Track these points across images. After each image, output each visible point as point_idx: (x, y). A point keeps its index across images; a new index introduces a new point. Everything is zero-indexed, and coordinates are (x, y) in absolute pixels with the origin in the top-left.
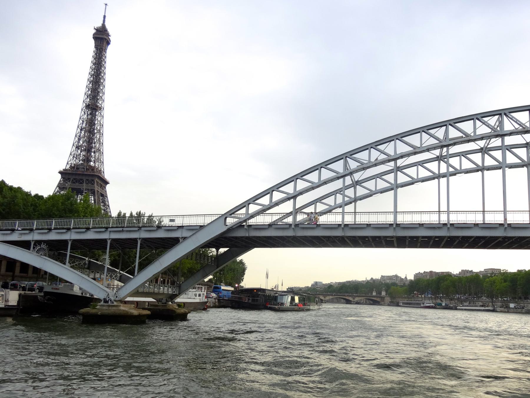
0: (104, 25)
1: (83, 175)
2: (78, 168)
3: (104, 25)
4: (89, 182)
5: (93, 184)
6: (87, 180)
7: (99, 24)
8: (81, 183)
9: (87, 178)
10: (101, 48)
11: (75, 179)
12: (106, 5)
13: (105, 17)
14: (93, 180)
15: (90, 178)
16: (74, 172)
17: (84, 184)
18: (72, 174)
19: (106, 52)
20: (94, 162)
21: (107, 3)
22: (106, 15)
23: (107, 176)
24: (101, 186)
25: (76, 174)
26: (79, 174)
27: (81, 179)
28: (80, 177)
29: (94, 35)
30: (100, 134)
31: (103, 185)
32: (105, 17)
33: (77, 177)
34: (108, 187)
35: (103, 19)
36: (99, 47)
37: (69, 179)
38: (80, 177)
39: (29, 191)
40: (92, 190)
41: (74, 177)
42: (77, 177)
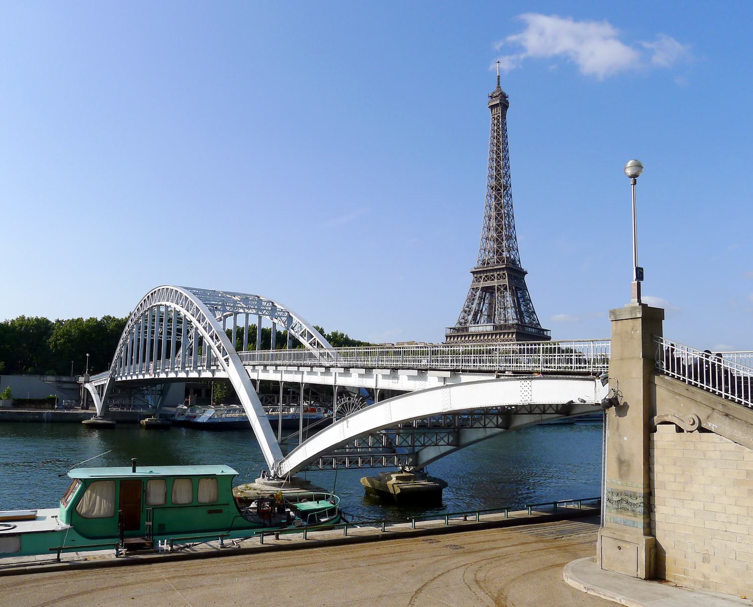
1: (493, 270)
2: (488, 263)
4: (500, 277)
5: (505, 279)
6: (498, 275)
8: (493, 280)
9: (498, 273)
10: (498, 116)
11: (486, 276)
14: (504, 274)
16: (485, 269)
17: (496, 280)
18: (483, 272)
19: (505, 119)
20: (509, 252)
23: (524, 266)
24: (517, 278)
25: (486, 271)
26: (490, 271)
27: (493, 275)
28: (492, 274)
30: (509, 218)
31: (519, 277)
34: (526, 278)
35: (497, 80)
36: (496, 116)
37: (481, 277)
40: (504, 285)
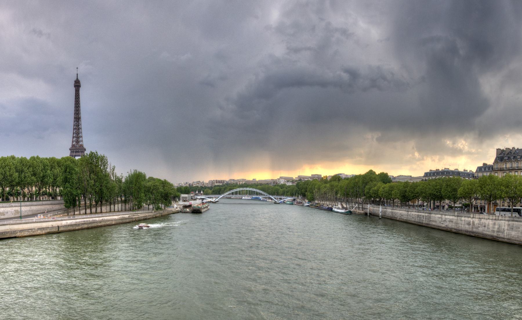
0: (77, 78)
3: (77, 78)
6: (81, 151)
7: (75, 79)
12: (77, 68)
13: (77, 74)
15: (82, 150)
21: (77, 67)
22: (78, 73)
27: (79, 151)
28: (78, 150)
29: (74, 84)
32: (77, 74)
33: (77, 150)
38: (78, 150)
39: (133, 172)
41: (75, 150)
42: (77, 150)
